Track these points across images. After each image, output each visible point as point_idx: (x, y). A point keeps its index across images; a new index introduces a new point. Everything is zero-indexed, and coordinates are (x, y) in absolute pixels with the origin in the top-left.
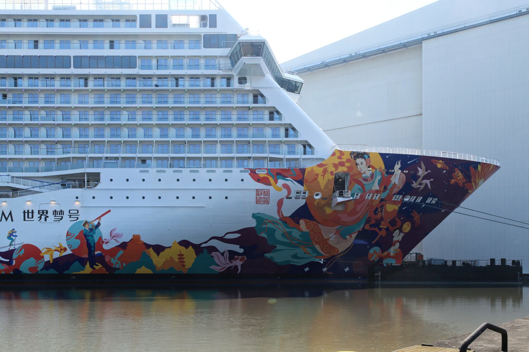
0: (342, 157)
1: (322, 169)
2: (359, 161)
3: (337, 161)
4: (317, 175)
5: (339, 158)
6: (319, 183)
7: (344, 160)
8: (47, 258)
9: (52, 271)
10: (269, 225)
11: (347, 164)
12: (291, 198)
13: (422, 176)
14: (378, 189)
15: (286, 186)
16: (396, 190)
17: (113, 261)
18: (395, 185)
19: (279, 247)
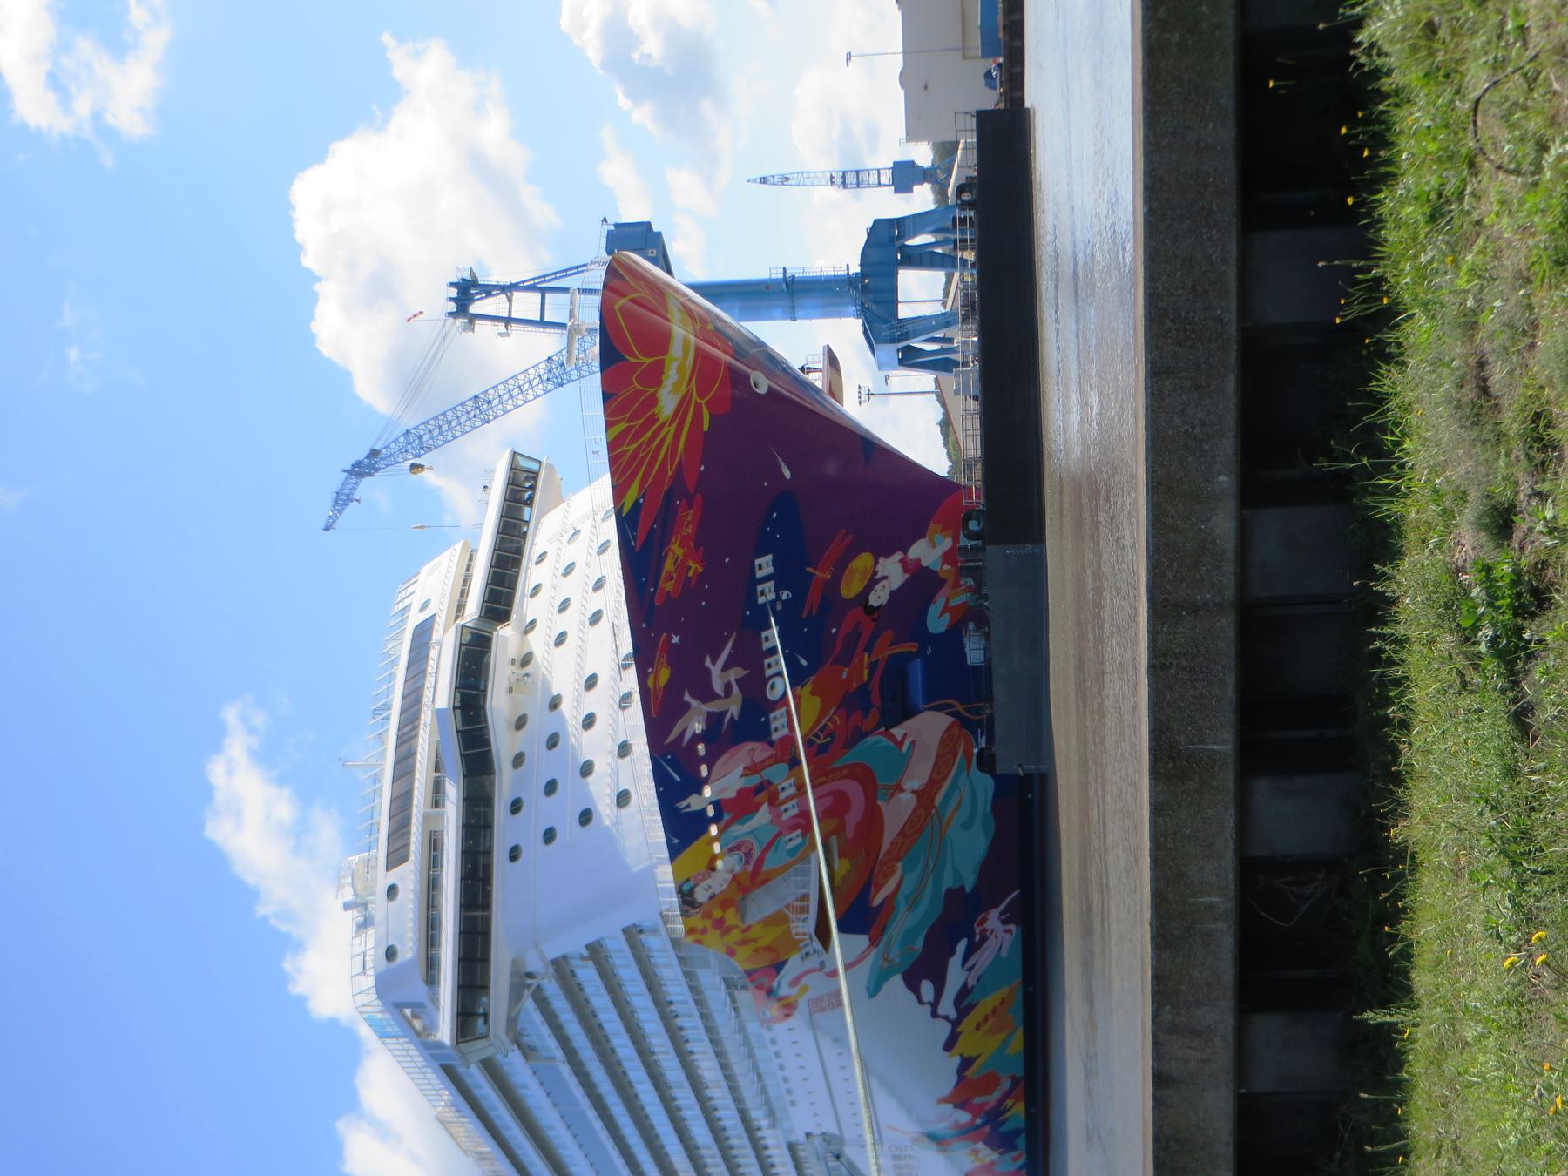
2: (701, 895)
3: (713, 935)
4: (756, 950)
5: (704, 931)
7: (708, 923)
8: (995, 1156)
9: (1021, 1141)
10: (895, 953)
11: (717, 913)
12: (822, 964)
14: (765, 806)
15: (795, 982)
16: (759, 751)
17: (997, 1095)
18: (751, 770)
19: (948, 882)
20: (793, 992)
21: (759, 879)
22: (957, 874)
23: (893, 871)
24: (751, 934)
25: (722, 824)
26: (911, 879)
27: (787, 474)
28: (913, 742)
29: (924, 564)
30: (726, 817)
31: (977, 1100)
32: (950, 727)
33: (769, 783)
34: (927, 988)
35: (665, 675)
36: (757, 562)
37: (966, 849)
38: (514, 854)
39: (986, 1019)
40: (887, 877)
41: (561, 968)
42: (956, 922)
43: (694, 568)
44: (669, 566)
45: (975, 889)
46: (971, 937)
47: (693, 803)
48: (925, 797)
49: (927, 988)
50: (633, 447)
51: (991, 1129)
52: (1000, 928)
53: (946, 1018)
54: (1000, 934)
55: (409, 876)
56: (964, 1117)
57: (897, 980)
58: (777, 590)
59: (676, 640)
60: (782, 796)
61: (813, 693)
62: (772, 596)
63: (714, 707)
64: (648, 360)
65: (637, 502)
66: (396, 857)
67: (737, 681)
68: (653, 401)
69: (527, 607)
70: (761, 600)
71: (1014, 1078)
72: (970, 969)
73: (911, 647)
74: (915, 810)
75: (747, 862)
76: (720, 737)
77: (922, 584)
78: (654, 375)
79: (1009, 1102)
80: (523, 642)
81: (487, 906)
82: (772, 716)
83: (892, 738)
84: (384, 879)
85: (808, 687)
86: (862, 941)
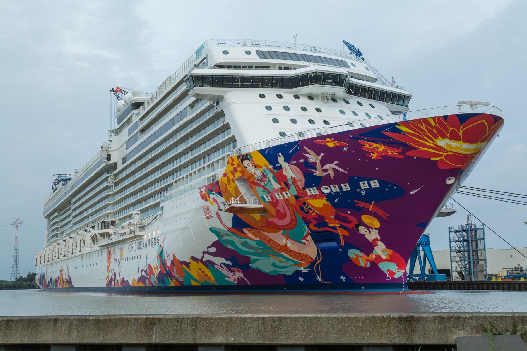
0: (234, 163)
1: (226, 178)
2: (246, 163)
3: (231, 168)
4: (226, 185)
5: (232, 164)
6: (229, 191)
7: (235, 166)
9: (161, 285)
10: (226, 238)
12: (221, 210)
13: (318, 162)
14: (280, 186)
15: (214, 199)
16: (301, 184)
17: (177, 276)
18: (294, 180)
19: (253, 257)
20: (211, 199)
21: (252, 185)
22: (256, 261)
23: (256, 236)
24: (231, 182)
25: (273, 170)
26: (253, 244)
27: (412, 193)
28: (305, 244)
29: (375, 248)
30: (275, 171)
31: (175, 269)
32: (311, 258)
33: (289, 188)
34: (213, 250)
35: (331, 145)
36: (376, 181)
37: (264, 265)
38: (262, 96)
39: (203, 272)
40: (254, 234)
41: (221, 115)
42: (239, 261)
43: (374, 156)
44: (375, 145)
45: (250, 267)
46: (233, 266)
47: (281, 159)
48: (285, 248)
49: (213, 250)
50: (425, 129)
51: (165, 274)
52: (236, 277)
53: (203, 257)
54: (234, 277)
55: (254, 58)
56: (169, 264)
57: (216, 239)
58: (365, 190)
59: (345, 149)
60: (284, 193)
61: (324, 204)
62: (363, 187)
63: (319, 165)
64: (461, 134)
65: (402, 131)
66: (261, 54)
67: (329, 174)
68: (444, 136)
69: (354, 100)
70: (361, 183)
71: (181, 283)
72: (221, 266)
73: (342, 243)
74: (279, 245)
75: (258, 180)
76: (307, 168)
77: (367, 247)
78: (454, 137)
79: (174, 280)
80: (340, 99)
81: (243, 86)
82: (315, 188)
83: (307, 236)
84: (253, 50)
85: (326, 203)
86: (230, 225)
